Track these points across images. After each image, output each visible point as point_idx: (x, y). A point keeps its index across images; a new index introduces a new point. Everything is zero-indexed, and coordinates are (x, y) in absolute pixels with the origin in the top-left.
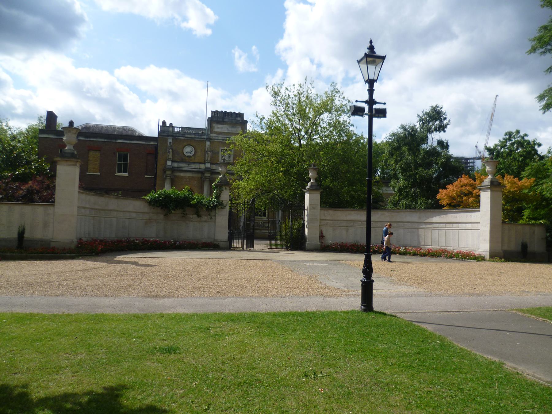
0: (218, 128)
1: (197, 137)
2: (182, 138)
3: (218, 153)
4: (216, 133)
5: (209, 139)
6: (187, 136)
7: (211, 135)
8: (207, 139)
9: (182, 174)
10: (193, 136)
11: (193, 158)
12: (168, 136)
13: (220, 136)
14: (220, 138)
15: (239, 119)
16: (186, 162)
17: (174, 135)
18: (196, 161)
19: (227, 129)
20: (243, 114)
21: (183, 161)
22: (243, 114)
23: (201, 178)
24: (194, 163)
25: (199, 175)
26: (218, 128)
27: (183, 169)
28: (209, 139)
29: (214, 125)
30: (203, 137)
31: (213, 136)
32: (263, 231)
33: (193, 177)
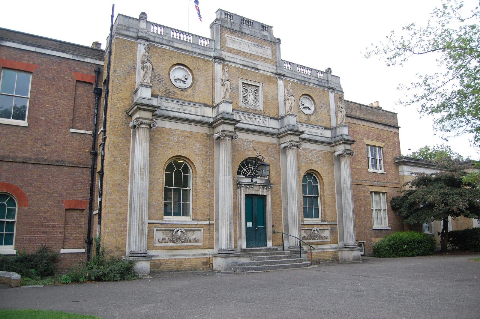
0: (234, 43)
1: (197, 51)
2: (167, 48)
4: (230, 50)
5: (219, 59)
6: (176, 45)
7: (222, 52)
8: (215, 58)
9: (168, 125)
10: (190, 48)
11: (190, 91)
12: (138, 38)
13: (238, 57)
14: (238, 62)
15: (266, 34)
16: (177, 100)
17: (152, 39)
18: (197, 100)
19: (249, 47)
20: (272, 27)
21: (169, 95)
22: (272, 27)
23: (209, 136)
24: (193, 103)
25: (204, 130)
26: (234, 42)
27: (172, 114)
28: (219, 59)
29: (226, 35)
30: (207, 53)
31: (226, 55)
32: (320, 247)
33: (191, 133)
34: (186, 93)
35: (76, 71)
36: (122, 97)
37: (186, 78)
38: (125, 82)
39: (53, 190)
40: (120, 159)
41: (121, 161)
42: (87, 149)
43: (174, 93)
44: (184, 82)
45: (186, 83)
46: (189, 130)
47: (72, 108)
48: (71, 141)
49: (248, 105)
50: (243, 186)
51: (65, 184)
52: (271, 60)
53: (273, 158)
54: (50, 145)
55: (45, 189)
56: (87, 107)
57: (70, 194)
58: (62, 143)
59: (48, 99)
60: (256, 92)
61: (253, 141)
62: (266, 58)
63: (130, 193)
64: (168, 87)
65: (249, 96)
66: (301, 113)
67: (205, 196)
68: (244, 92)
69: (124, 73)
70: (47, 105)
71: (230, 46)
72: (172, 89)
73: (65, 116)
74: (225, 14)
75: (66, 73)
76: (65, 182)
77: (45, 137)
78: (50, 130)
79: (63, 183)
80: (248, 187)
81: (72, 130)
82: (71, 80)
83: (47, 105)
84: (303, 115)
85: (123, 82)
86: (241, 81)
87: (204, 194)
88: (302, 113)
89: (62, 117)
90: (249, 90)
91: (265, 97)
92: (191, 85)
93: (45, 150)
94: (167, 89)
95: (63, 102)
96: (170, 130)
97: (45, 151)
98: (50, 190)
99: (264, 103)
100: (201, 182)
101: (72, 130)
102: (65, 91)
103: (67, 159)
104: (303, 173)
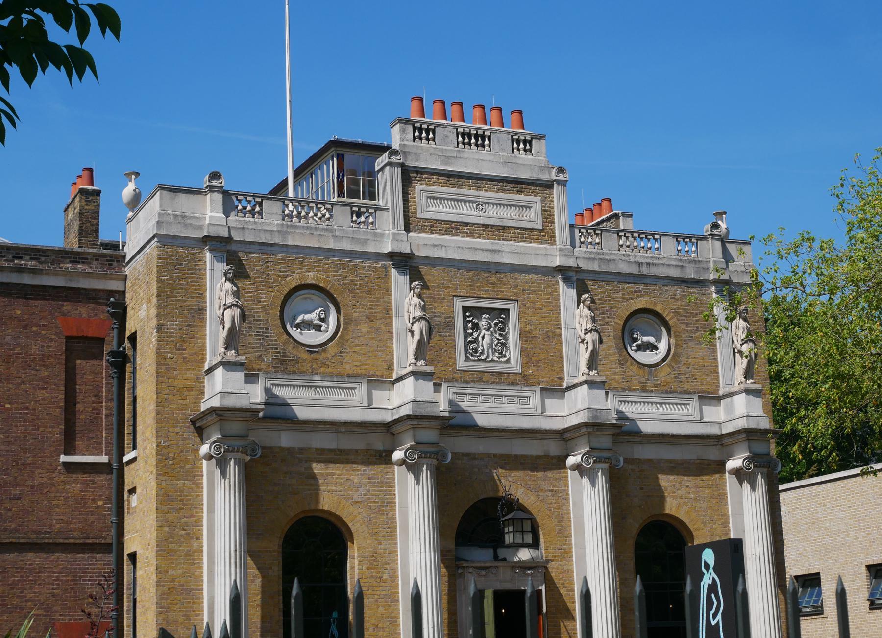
3: (451, 325)
11: (332, 348)
18: (348, 369)
34: (323, 356)
35: (64, 315)
36: (181, 386)
37: (323, 316)
38: (185, 350)
39: (32, 601)
40: (184, 529)
41: (184, 532)
42: (100, 500)
43: (296, 361)
44: (318, 328)
45: (323, 328)
46: (333, 446)
47: (62, 404)
48: (65, 484)
49: (482, 364)
50: (471, 570)
51: (58, 584)
52: (541, 231)
53: (550, 494)
54: (19, 498)
55: (16, 601)
56: (93, 398)
57: (69, 608)
58: (45, 490)
59: (8, 391)
60: (502, 328)
61: (495, 455)
62: (526, 229)
63: (208, 600)
64: (280, 348)
65: (483, 338)
66: (629, 363)
67: (377, 601)
68: (470, 331)
69: (180, 329)
70: (8, 406)
71: (428, 216)
72: (291, 352)
73: (46, 427)
74: (414, 128)
75: (42, 322)
76: (56, 580)
77: (9, 479)
78: (17, 463)
79: (53, 584)
80: (483, 573)
81: (63, 458)
82: (53, 337)
83: (8, 406)
84: (635, 368)
85: (179, 349)
86: (459, 305)
87: (376, 597)
88: (631, 365)
89: (41, 429)
90: (483, 323)
91: (525, 336)
92: (336, 333)
93: (10, 510)
94: (279, 353)
95: (41, 394)
96: (290, 450)
97: (9, 514)
98: (27, 601)
99: (524, 352)
100: (368, 569)
101: (63, 458)
102: (44, 366)
103: (58, 526)
104: (634, 526)
